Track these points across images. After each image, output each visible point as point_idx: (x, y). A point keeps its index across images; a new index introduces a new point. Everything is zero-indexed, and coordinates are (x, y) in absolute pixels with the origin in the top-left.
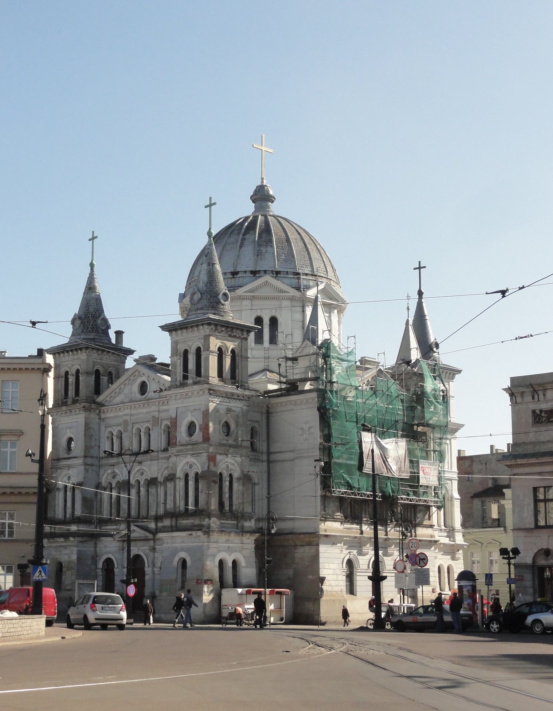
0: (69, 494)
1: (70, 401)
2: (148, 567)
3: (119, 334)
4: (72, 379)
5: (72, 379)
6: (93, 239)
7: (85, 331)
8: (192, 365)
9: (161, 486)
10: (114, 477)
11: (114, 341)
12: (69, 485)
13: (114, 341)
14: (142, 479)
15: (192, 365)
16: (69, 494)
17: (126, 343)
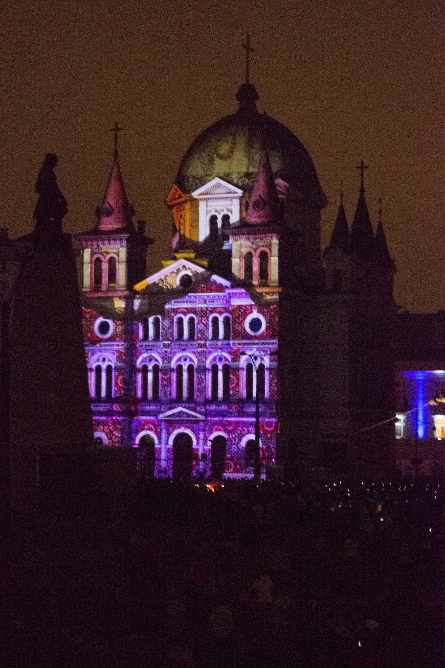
0: (104, 375)
1: (104, 288)
2: (198, 444)
3: (142, 224)
4: (105, 266)
5: (105, 266)
6: (116, 129)
7: (117, 220)
8: (256, 268)
9: (209, 372)
10: (150, 360)
11: (137, 230)
12: (104, 366)
13: (137, 230)
14: (185, 365)
15: (256, 268)
16: (104, 375)
17: (148, 233)
